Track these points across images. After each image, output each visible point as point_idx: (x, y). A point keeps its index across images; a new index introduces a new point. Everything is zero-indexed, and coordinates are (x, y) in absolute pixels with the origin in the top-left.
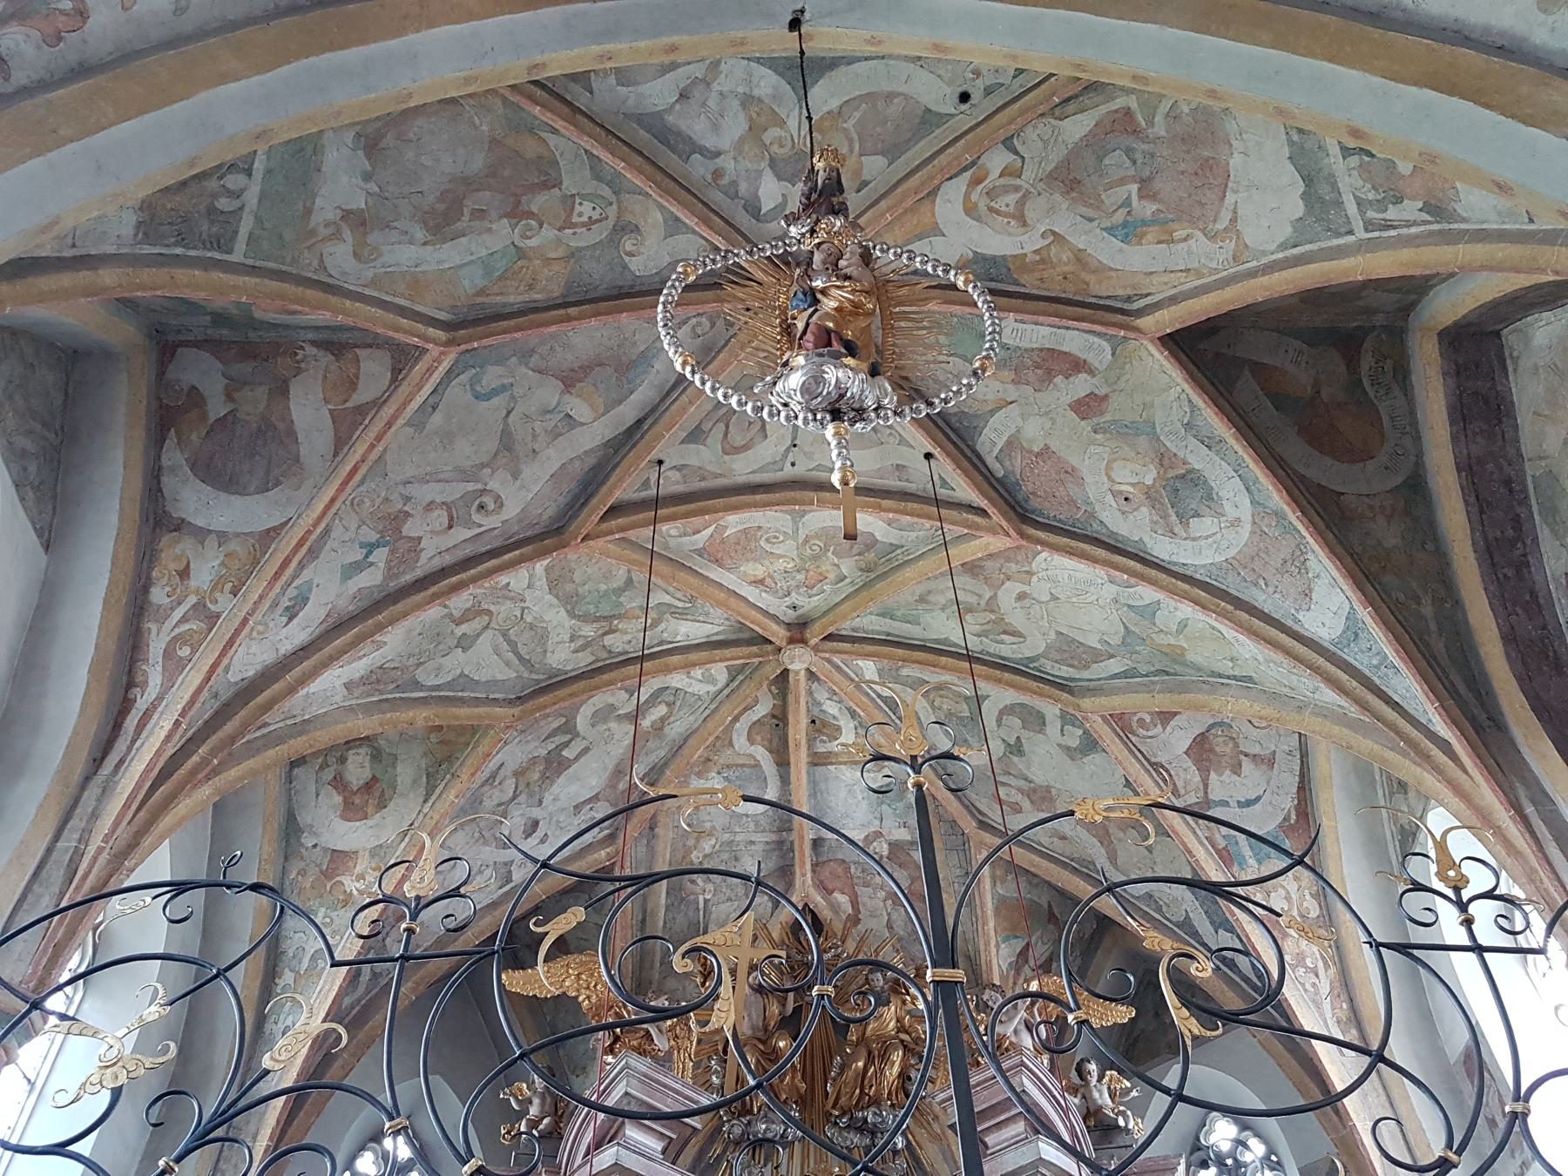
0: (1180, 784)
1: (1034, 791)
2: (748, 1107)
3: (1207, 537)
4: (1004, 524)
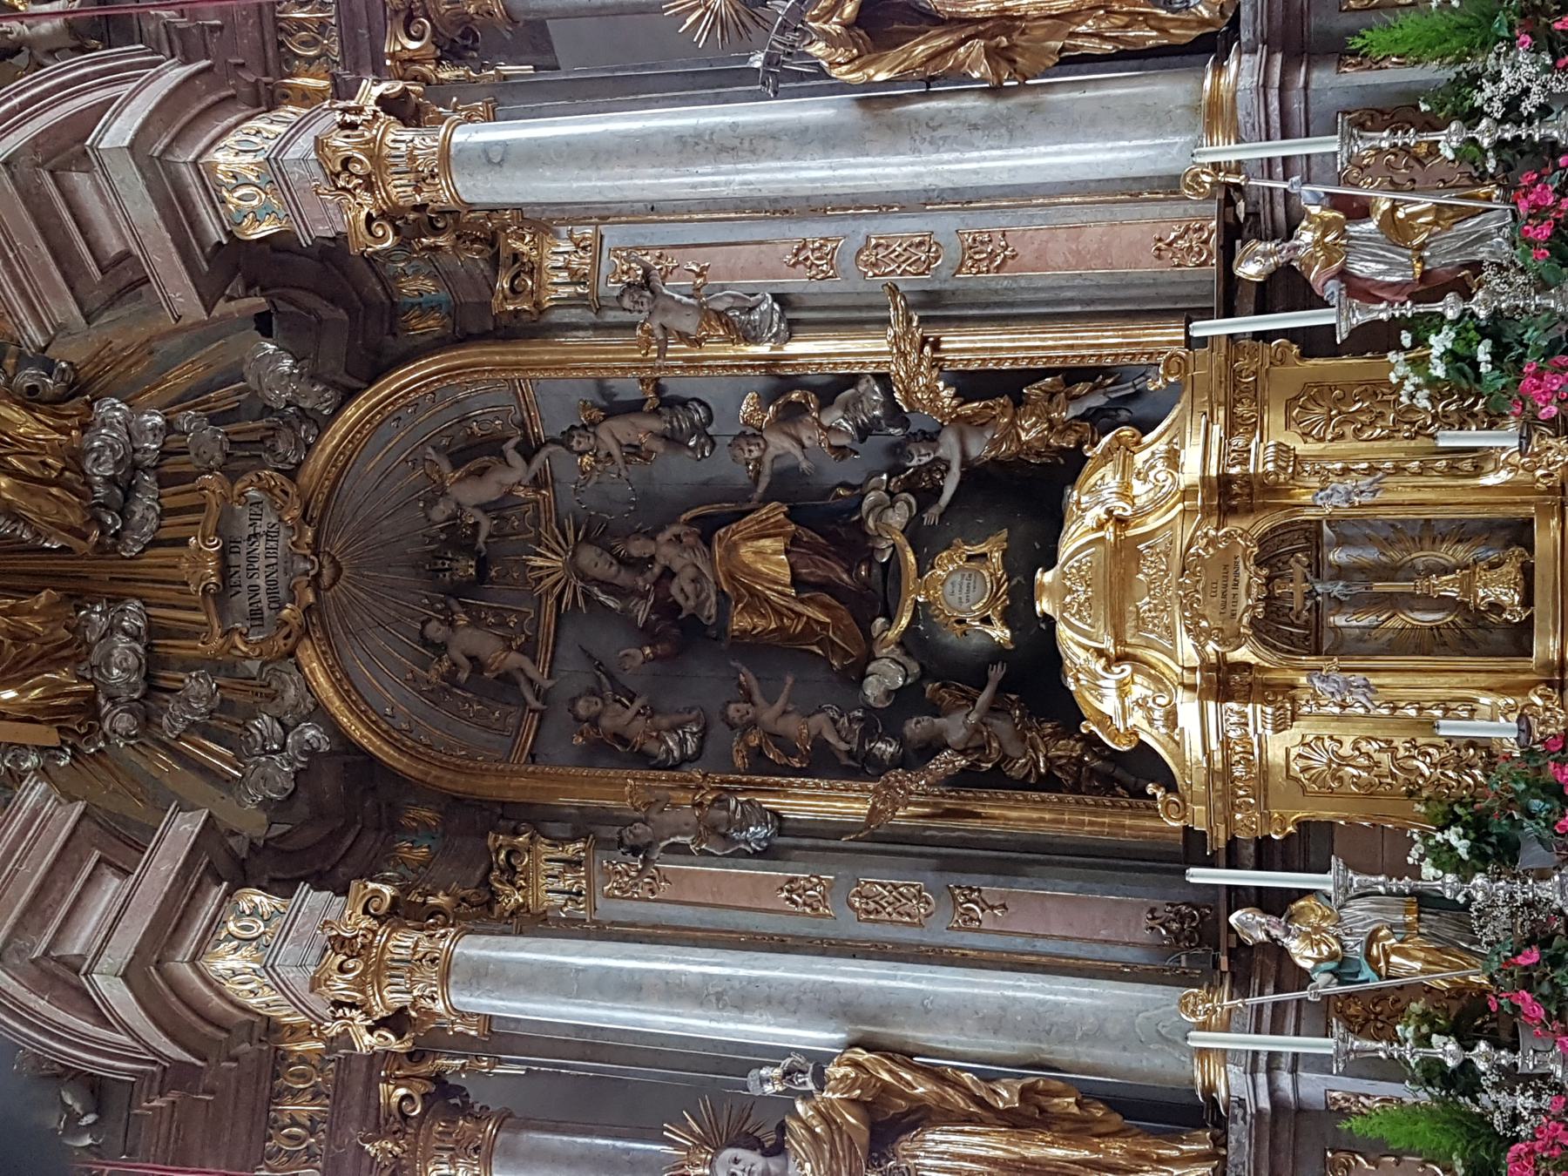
2: (80, 700)
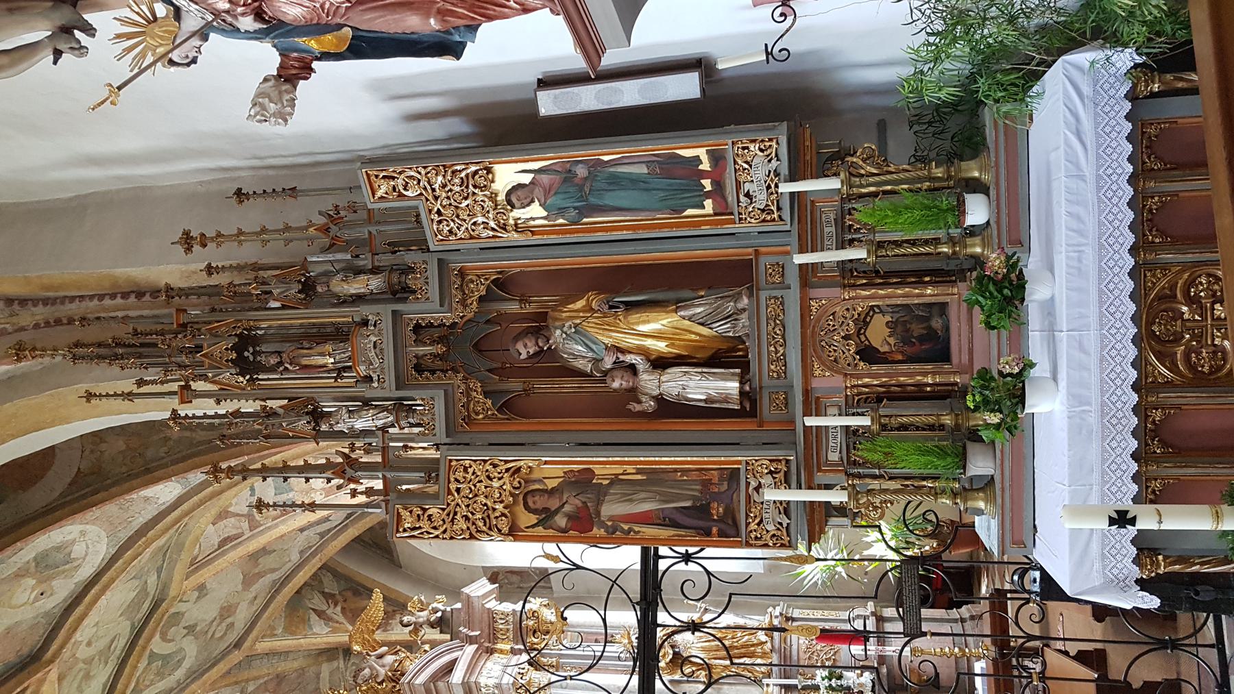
0: (234, 532)
1: (221, 616)
3: (88, 548)
4: (39, 675)
